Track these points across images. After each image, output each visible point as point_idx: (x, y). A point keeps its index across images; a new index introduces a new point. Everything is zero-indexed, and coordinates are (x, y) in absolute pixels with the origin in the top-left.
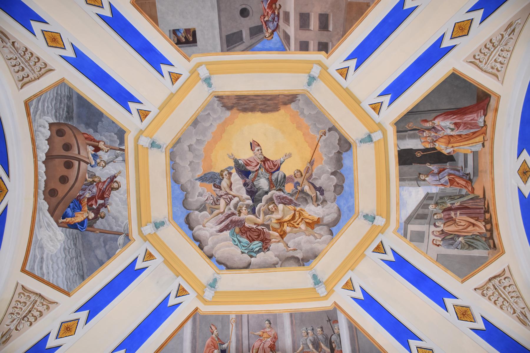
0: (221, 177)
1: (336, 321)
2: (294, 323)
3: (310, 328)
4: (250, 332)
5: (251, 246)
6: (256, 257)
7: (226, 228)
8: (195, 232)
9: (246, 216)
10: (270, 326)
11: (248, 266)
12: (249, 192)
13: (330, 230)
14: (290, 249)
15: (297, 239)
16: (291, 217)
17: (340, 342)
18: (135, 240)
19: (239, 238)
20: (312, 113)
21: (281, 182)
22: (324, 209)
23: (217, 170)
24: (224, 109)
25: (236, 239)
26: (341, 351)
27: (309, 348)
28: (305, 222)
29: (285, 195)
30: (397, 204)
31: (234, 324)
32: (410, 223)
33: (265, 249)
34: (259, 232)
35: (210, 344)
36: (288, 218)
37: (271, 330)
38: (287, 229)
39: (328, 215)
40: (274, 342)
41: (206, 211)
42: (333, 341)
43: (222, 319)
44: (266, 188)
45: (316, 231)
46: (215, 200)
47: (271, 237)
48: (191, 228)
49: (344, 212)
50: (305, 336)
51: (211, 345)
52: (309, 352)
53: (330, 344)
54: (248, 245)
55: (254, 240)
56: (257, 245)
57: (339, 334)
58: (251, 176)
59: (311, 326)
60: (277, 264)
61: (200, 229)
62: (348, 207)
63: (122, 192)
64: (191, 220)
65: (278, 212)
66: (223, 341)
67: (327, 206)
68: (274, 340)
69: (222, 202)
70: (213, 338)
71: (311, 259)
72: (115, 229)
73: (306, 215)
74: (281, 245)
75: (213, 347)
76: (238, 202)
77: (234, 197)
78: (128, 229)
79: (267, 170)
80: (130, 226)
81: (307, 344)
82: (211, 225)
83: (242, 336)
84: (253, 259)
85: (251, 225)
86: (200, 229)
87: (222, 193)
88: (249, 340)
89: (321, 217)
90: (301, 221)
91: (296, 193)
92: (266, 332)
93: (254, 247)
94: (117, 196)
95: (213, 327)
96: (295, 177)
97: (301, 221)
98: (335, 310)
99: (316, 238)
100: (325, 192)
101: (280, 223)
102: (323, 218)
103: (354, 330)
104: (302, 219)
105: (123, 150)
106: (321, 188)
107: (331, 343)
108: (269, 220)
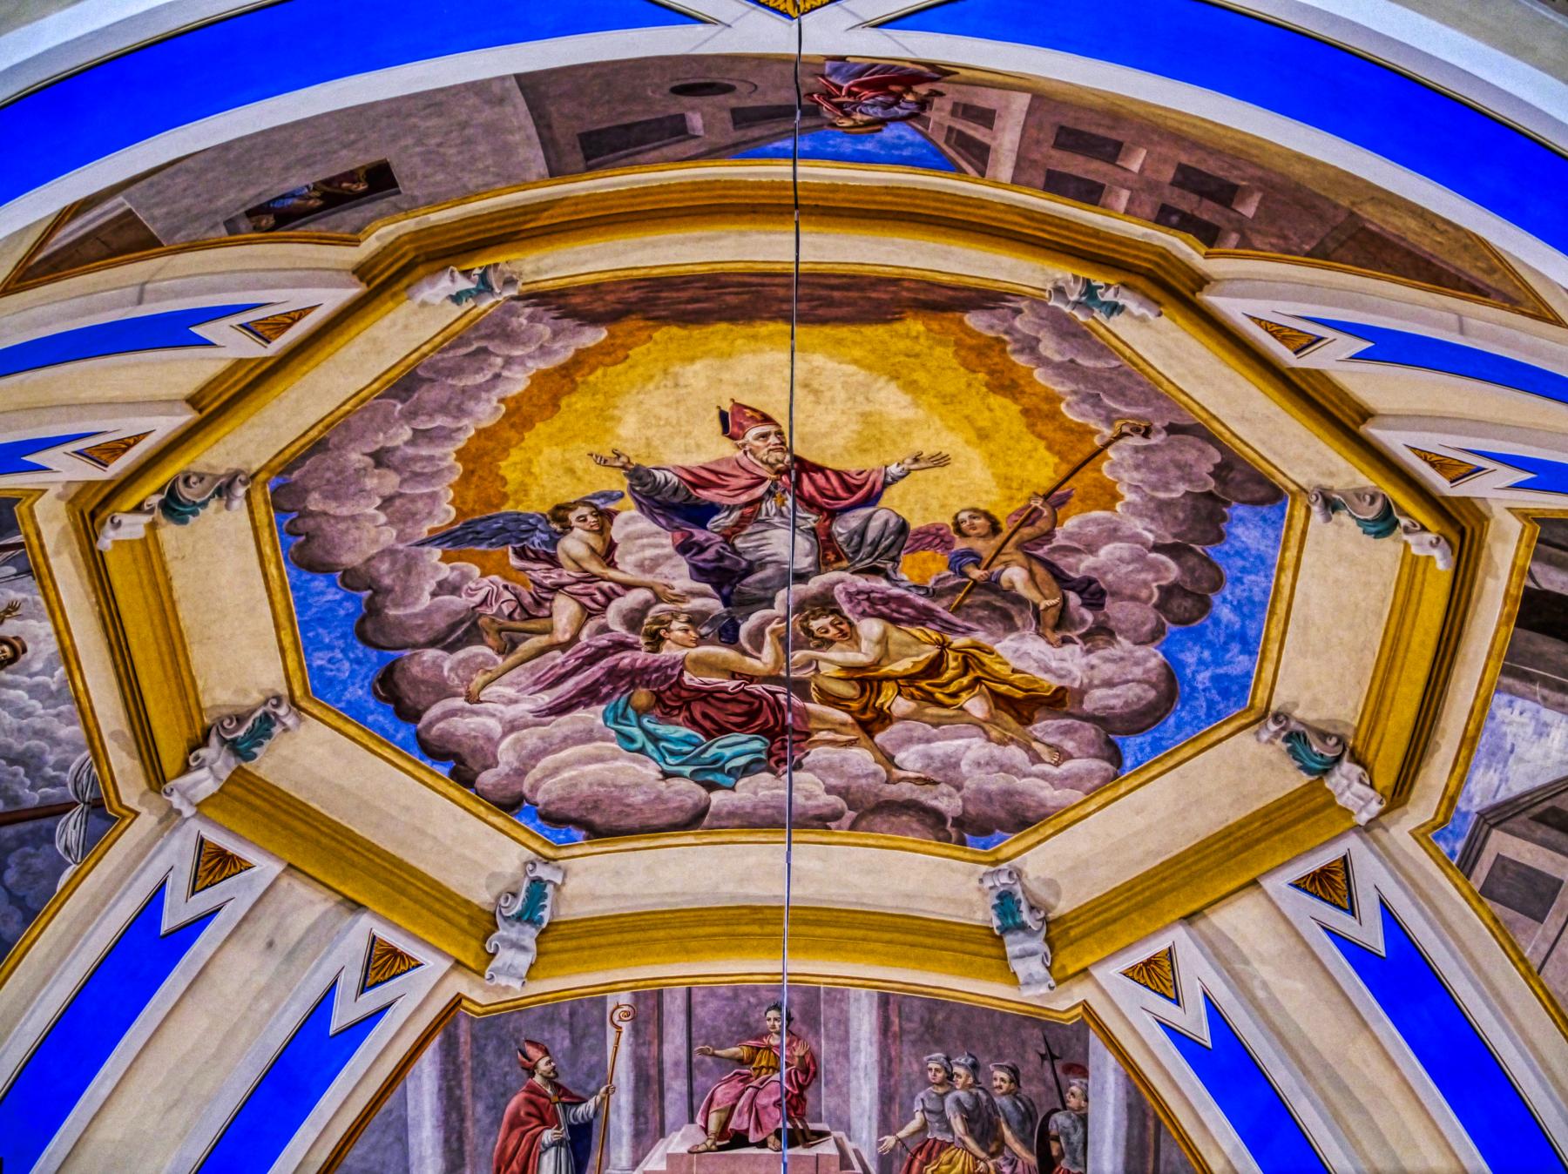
0: (555, 526)
1: (1081, 1070)
2: (896, 1028)
5: (713, 750)
6: (733, 789)
7: (588, 696)
8: (431, 724)
9: (685, 651)
11: (694, 820)
12: (699, 573)
13: (1110, 743)
14: (902, 774)
15: (940, 748)
16: (920, 668)
18: (137, 814)
19: (651, 726)
20: (1080, 361)
21: (882, 546)
22: (1093, 659)
23: (536, 504)
24: (566, 323)
25: (635, 731)
27: (950, 1129)
28: (991, 690)
29: (896, 591)
30: (1469, 742)
31: (626, 1027)
32: (1508, 825)
33: (777, 763)
34: (751, 704)
36: (902, 666)
38: (902, 705)
39: (1109, 683)
40: (802, 1088)
41: (483, 642)
42: (1053, 1132)
43: (572, 1014)
44: (804, 562)
45: (1038, 735)
46: (528, 600)
47: (813, 725)
48: (409, 714)
49: (1194, 689)
53: (1042, 1142)
54: (697, 746)
55: (723, 730)
56: (739, 746)
57: (1086, 1115)
58: (722, 520)
60: (837, 816)
61: (453, 713)
62: (1215, 679)
63: (37, 666)
64: (404, 686)
65: (857, 643)
67: (1115, 651)
69: (564, 611)
70: (533, 1090)
71: (1002, 829)
72: (32, 797)
73: (997, 667)
74: (860, 759)
75: (535, 1122)
76: (647, 605)
77: (628, 587)
78: (95, 782)
79: (810, 504)
80: (105, 768)
81: (941, 1113)
82: (511, 692)
84: (717, 798)
85: (715, 680)
86: (453, 713)
87: (568, 573)
89: (1076, 685)
90: (971, 687)
91: (955, 589)
93: (728, 752)
94: (15, 686)
95: (532, 1051)
96: (959, 530)
97: (971, 687)
98: (1080, 1030)
99: (1036, 758)
100: (1108, 600)
101: (859, 680)
102: (1081, 693)
103: (1151, 1124)
104: (978, 680)
105: (20, 545)
106: (1091, 581)
107: (1045, 1138)
108: (809, 664)
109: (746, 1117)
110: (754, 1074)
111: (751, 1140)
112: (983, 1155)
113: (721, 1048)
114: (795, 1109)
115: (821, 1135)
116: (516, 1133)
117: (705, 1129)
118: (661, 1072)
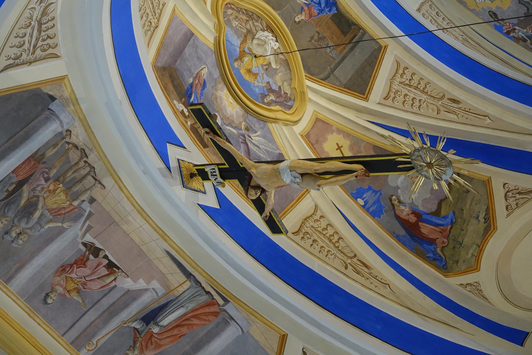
2: (17, 265)
3: (8, 238)
4: (85, 309)
10: (51, 292)
27: (42, 215)
35: (153, 347)
37: (56, 285)
40: (71, 266)
42: (6, 193)
51: (152, 344)
52: (48, 210)
59: (3, 239)
66: (133, 334)
75: (153, 339)
83: (100, 315)
88: (99, 300)
92: (65, 288)
109: (99, 271)
110: (79, 283)
111: (107, 261)
112: (41, 199)
113: (78, 302)
115: (85, 244)
116: (162, 342)
117: (115, 279)
118: (104, 312)
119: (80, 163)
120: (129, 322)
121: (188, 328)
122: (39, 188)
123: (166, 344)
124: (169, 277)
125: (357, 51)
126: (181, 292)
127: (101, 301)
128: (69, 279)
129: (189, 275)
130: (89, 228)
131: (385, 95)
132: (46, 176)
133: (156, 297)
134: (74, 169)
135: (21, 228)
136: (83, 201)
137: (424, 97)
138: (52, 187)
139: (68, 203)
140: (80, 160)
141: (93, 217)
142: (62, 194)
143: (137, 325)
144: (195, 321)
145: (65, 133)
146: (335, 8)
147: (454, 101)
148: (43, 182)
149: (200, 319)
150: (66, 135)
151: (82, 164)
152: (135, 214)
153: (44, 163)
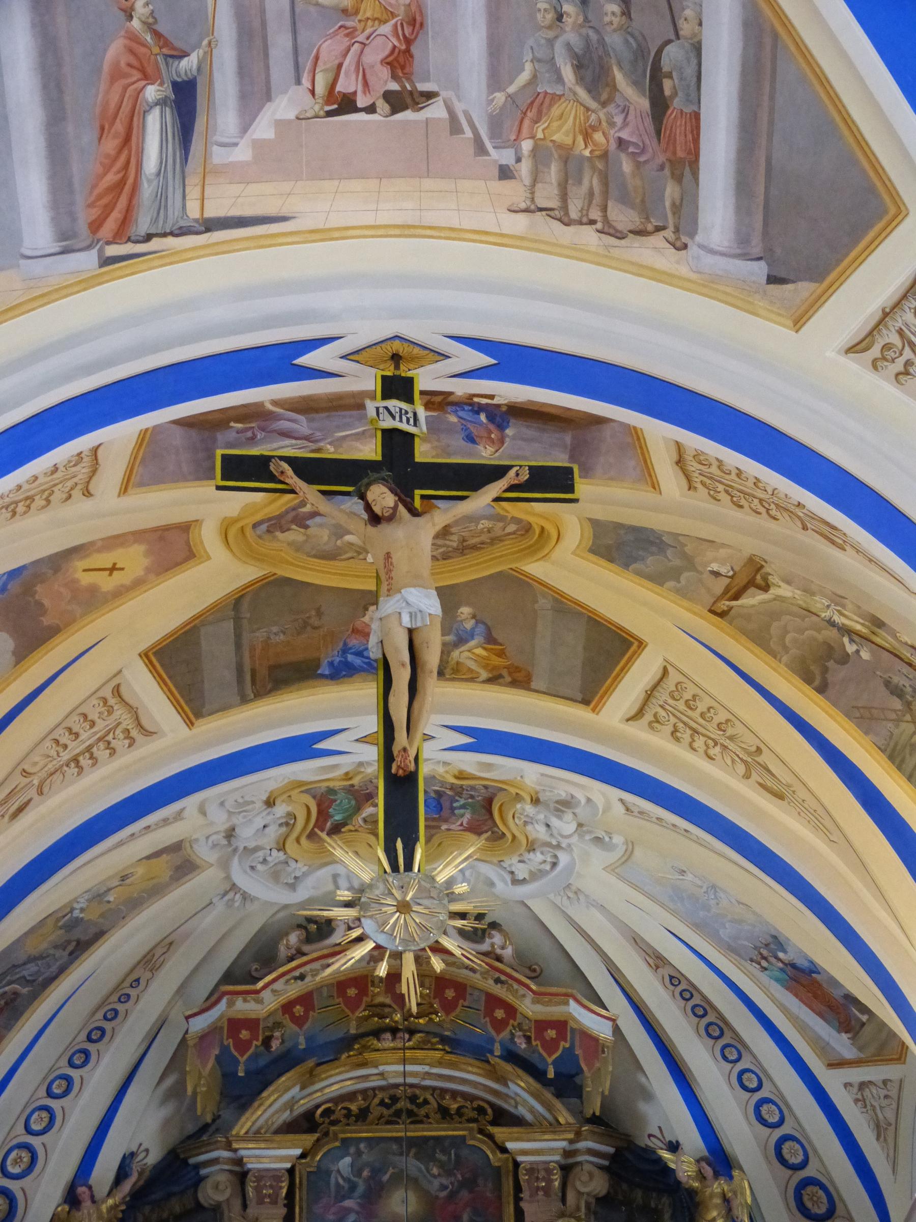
17: (695, 79)
26: (697, 116)
27: (560, 79)
35: (123, 64)
40: (408, 42)
42: (666, 68)
50: (549, 27)
51: (130, 65)
52: (560, 96)
57: (699, 43)
66: (178, 44)
68: (407, 31)
70: (133, 37)
75: (137, 75)
83: (263, 11)
88: (295, 32)
103: (768, 41)
107: (657, 76)
109: (353, 77)
111: (360, 104)
112: (593, 105)
114: (403, 68)
115: (429, 96)
116: (118, 87)
117: (313, 92)
118: (264, 24)
119: (600, 214)
120: (205, 53)
121: (107, 156)
122: (618, 120)
123: (107, 92)
124: (235, 189)
125: (229, 676)
126: (188, 190)
127: (289, 36)
128: (385, 16)
129: (210, 225)
130: (455, 127)
131: (123, 690)
132: (631, 150)
133: (216, 138)
134: (597, 199)
135: (567, 29)
136: (518, 160)
137: (66, 756)
138: (598, 137)
139: (540, 135)
140: (605, 217)
141: (471, 151)
142: (568, 141)
143: (189, 64)
144: (111, 178)
145: (685, 239)
146: (327, 672)
147: (20, 810)
148: (624, 135)
149: (109, 190)
150: (678, 239)
151: (595, 214)
152: (409, 218)
153: (662, 168)
